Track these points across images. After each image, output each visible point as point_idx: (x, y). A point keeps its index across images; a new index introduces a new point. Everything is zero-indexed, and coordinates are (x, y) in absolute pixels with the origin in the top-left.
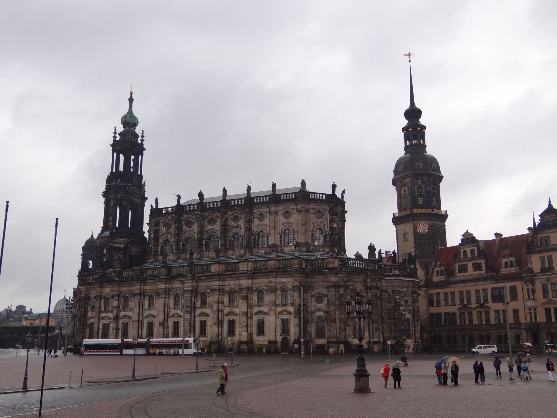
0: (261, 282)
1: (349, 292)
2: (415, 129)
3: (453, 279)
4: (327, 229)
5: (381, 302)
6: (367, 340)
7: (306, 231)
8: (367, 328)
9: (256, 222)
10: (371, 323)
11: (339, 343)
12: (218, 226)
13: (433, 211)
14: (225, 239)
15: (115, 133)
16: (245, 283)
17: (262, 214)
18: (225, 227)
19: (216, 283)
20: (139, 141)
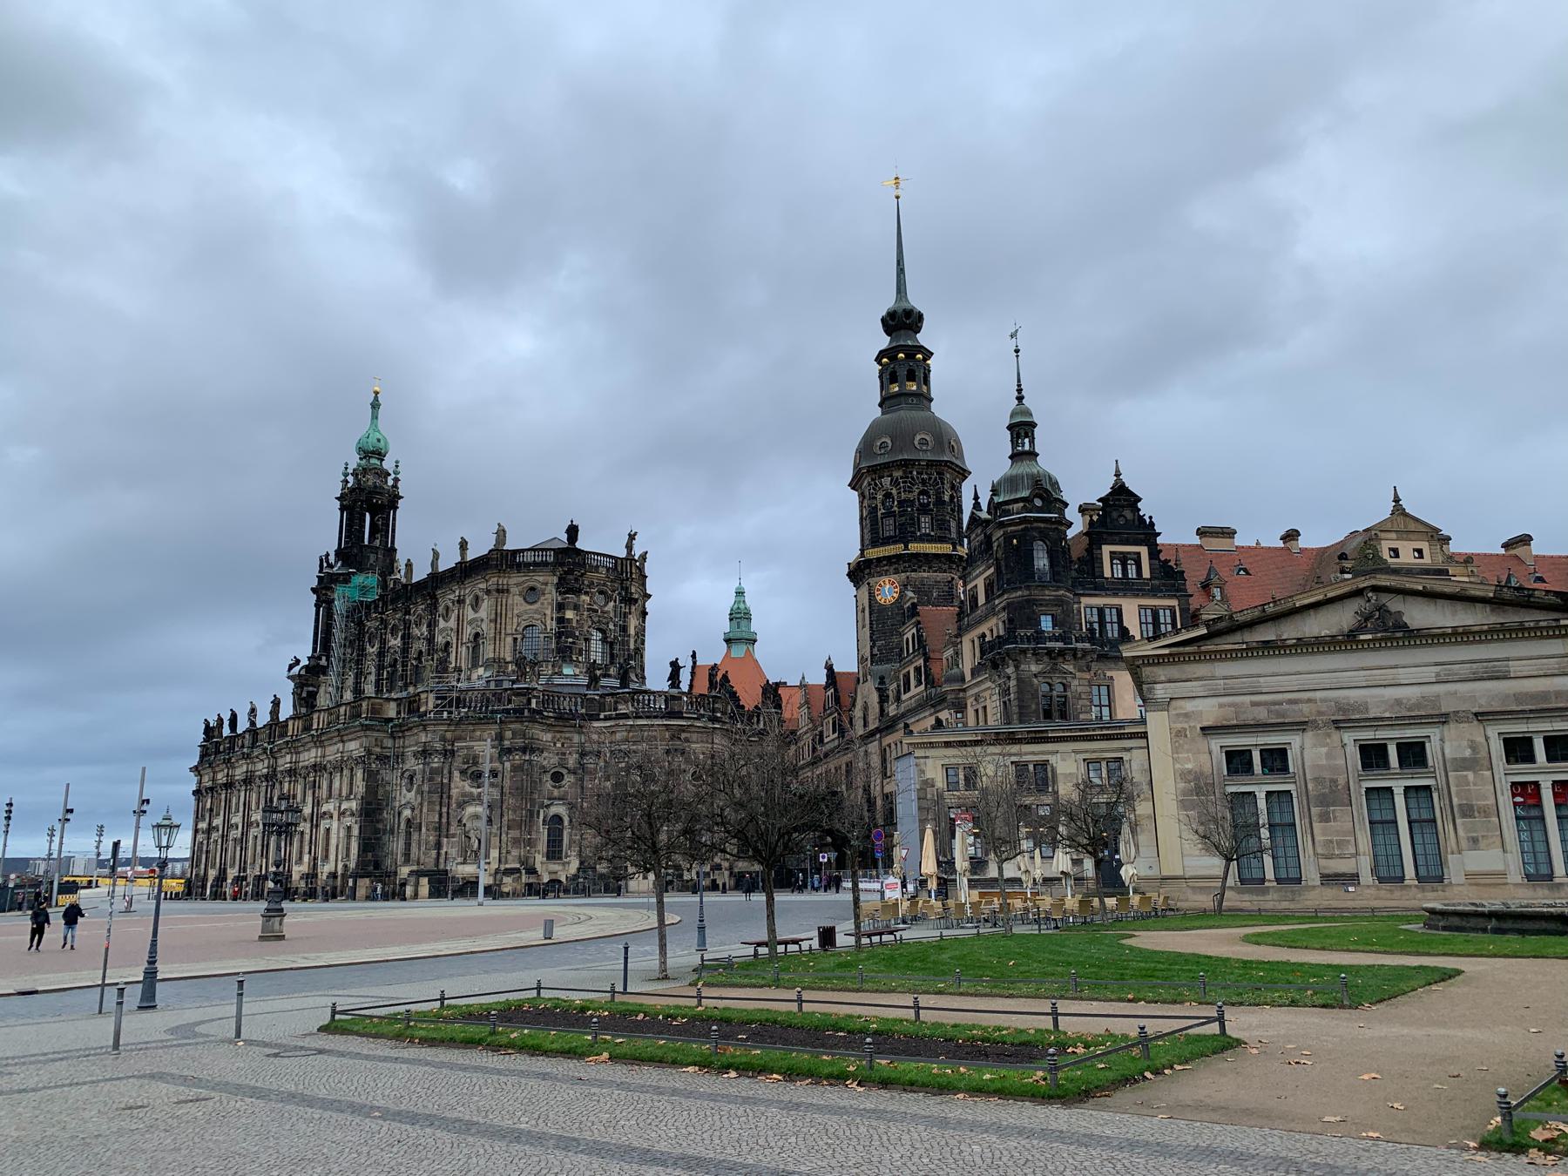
0: (333, 752)
1: (458, 762)
2: (893, 358)
3: (902, 710)
4: (552, 625)
5: (582, 780)
6: (495, 866)
7: (498, 632)
8: (495, 841)
9: (442, 624)
10: (505, 829)
11: (418, 874)
12: (395, 642)
13: (906, 548)
14: (404, 665)
15: (346, 475)
16: (310, 756)
17: (447, 608)
18: (407, 638)
19: (288, 758)
20: (390, 483)
